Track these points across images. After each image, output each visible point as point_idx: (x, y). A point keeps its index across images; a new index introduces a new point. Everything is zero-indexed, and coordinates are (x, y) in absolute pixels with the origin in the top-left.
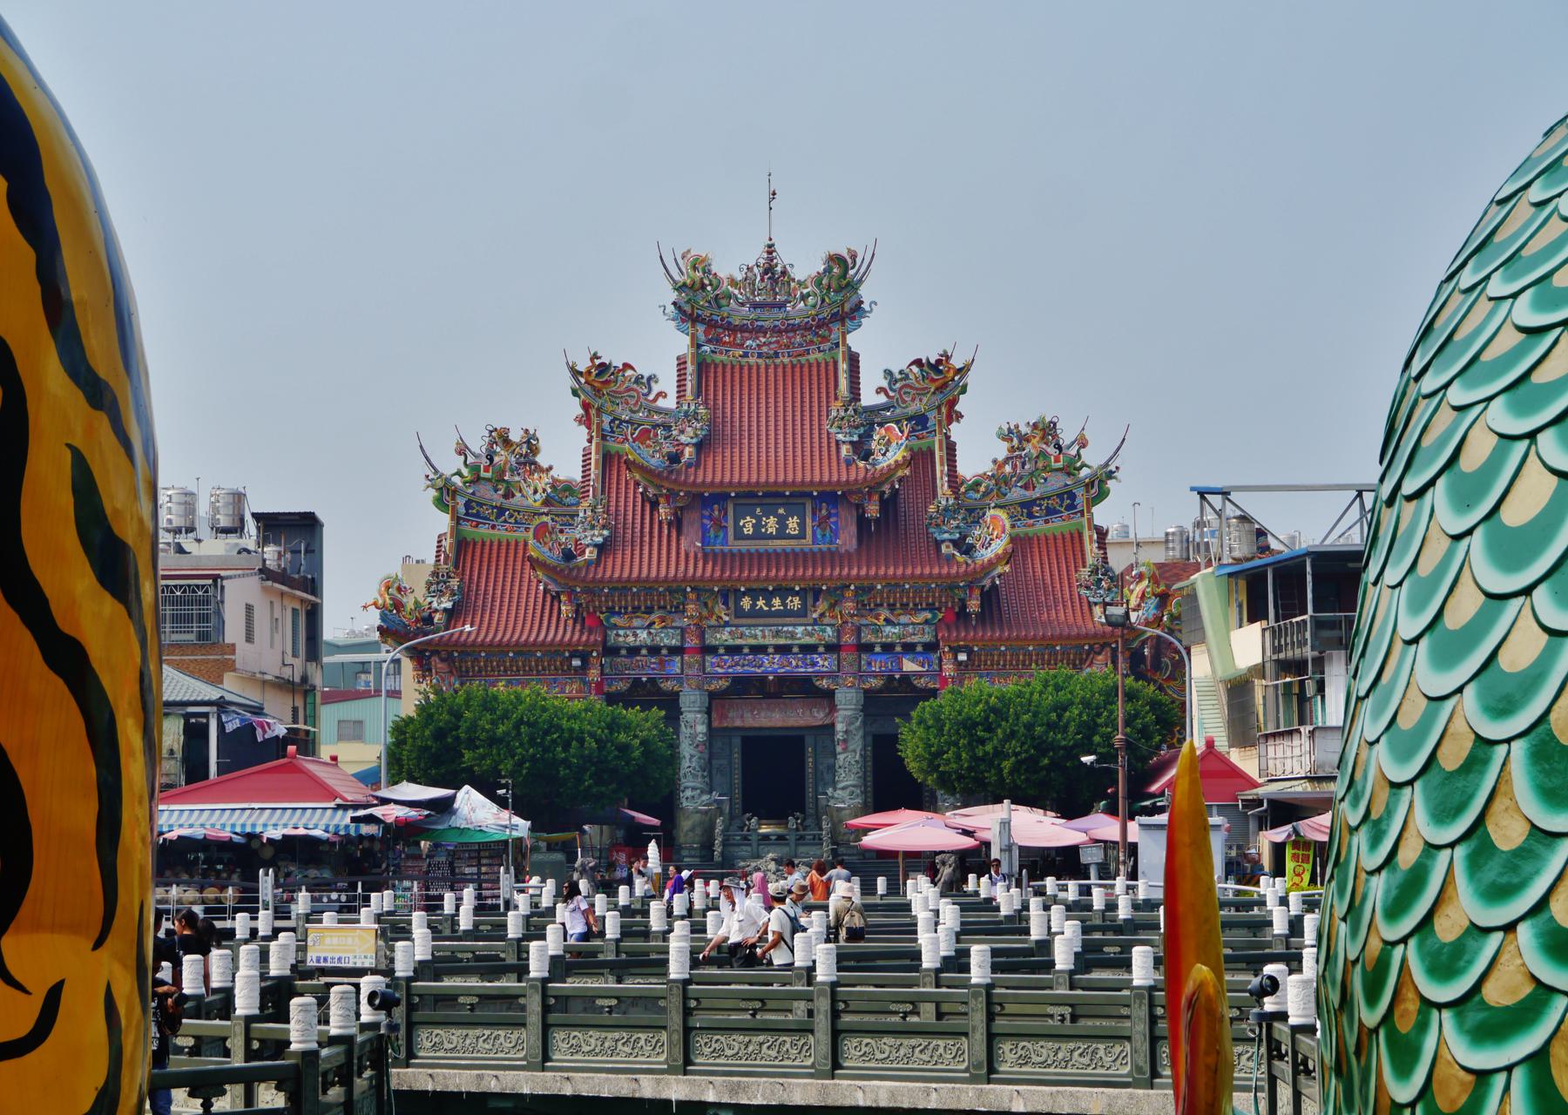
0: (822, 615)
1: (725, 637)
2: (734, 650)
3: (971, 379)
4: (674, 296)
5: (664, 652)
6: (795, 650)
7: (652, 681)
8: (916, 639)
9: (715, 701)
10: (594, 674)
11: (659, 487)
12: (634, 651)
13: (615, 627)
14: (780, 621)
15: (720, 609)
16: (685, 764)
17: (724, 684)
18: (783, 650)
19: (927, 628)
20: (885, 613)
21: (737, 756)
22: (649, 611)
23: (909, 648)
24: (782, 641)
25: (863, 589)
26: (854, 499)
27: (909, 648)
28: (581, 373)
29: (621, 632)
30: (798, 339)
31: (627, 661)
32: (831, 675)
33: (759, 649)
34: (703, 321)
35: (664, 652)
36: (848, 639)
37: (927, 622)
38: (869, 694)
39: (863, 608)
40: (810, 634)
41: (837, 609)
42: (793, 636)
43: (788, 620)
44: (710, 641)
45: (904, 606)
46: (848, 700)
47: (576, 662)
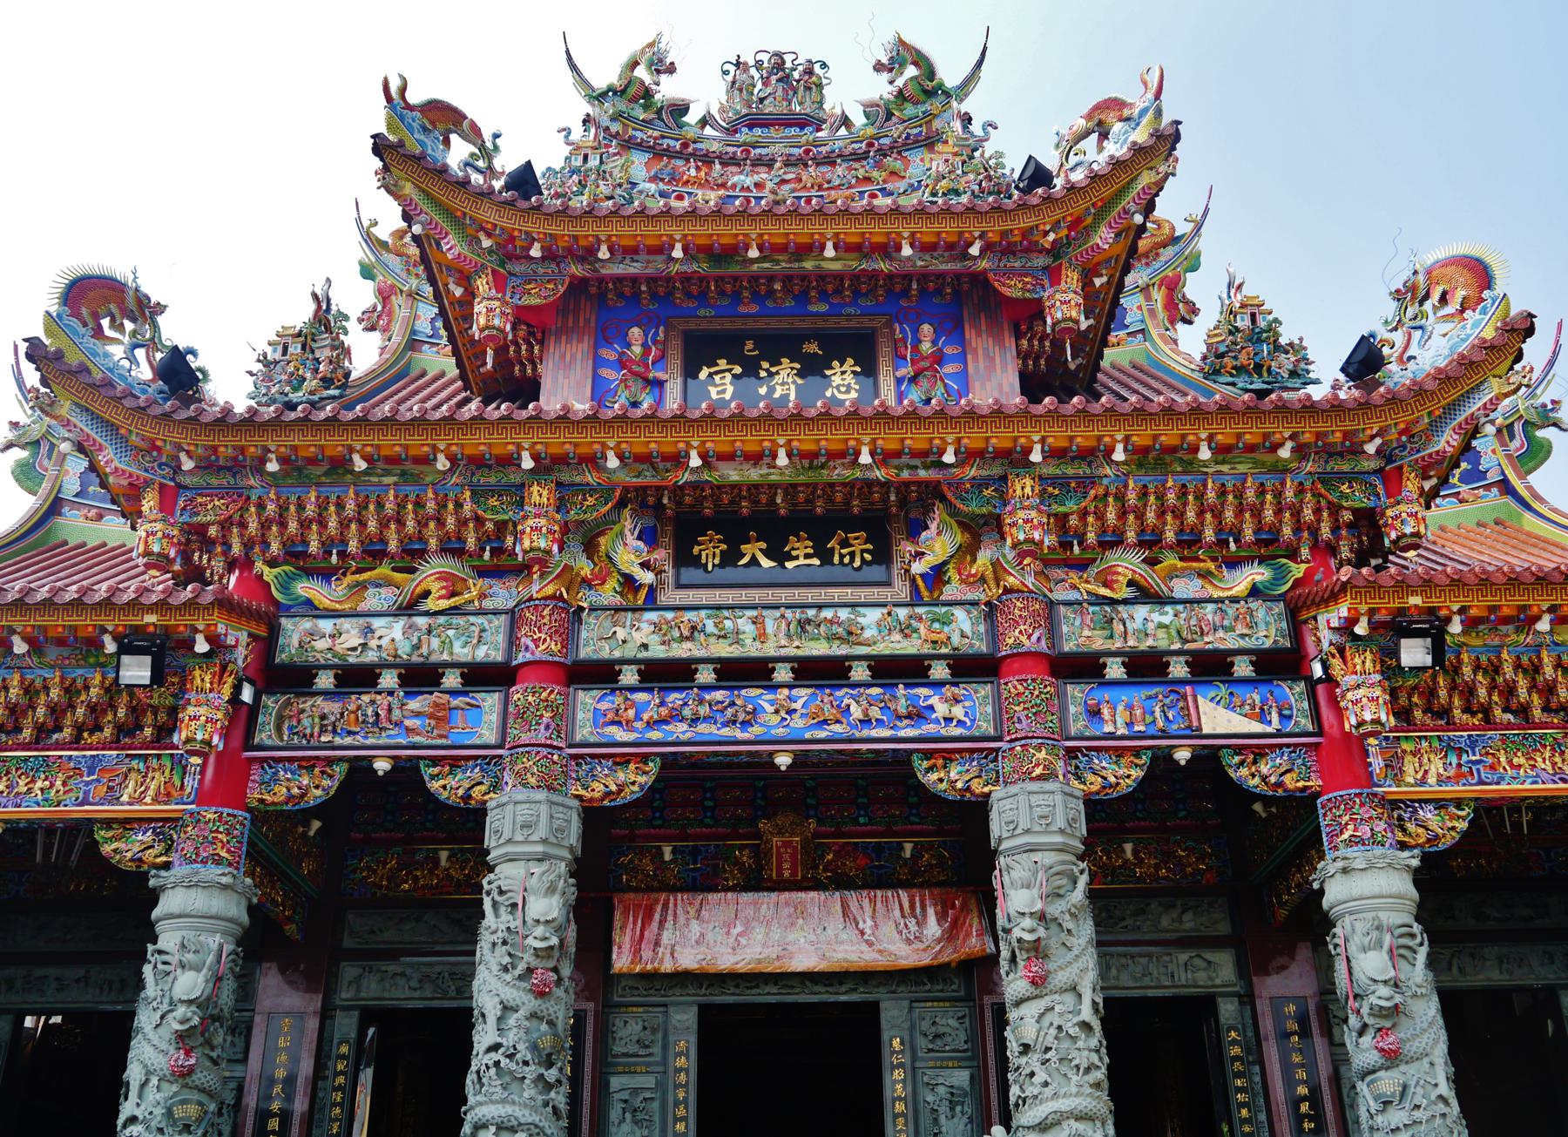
0: (937, 576)
1: (641, 637)
2: (666, 674)
3: (1204, 244)
4: (588, 109)
5: (452, 680)
6: (860, 672)
7: (407, 772)
8: (1230, 642)
9: (617, 862)
10: (202, 720)
11: (471, 230)
12: (356, 678)
13: (311, 609)
14: (810, 595)
15: (628, 552)
16: (483, 1036)
17: (635, 781)
18: (821, 673)
19: (1259, 609)
20: (1127, 563)
21: (685, 1061)
22: (412, 556)
23: (1211, 667)
24: (819, 649)
25: (1062, 482)
26: (1013, 289)
27: (1211, 667)
28: (384, 244)
29: (326, 625)
30: (839, 170)
31: (332, 708)
32: (982, 750)
33: (745, 672)
34: (641, 146)
35: (452, 680)
36: (1023, 637)
37: (1255, 592)
38: (1094, 806)
39: (1068, 552)
40: (906, 631)
41: (984, 557)
42: (850, 635)
43: (836, 594)
44: (593, 644)
45: (1188, 543)
46: (1035, 828)
47: (136, 671)
